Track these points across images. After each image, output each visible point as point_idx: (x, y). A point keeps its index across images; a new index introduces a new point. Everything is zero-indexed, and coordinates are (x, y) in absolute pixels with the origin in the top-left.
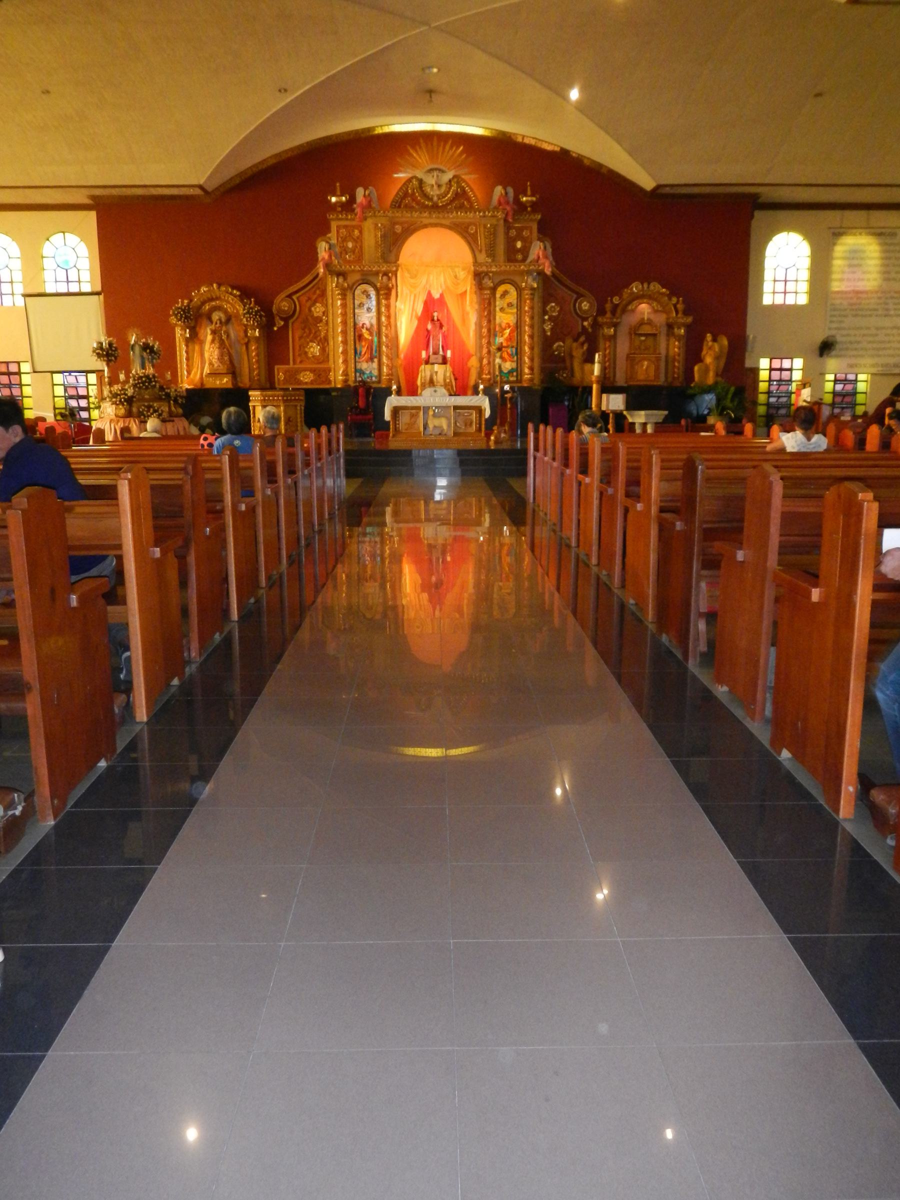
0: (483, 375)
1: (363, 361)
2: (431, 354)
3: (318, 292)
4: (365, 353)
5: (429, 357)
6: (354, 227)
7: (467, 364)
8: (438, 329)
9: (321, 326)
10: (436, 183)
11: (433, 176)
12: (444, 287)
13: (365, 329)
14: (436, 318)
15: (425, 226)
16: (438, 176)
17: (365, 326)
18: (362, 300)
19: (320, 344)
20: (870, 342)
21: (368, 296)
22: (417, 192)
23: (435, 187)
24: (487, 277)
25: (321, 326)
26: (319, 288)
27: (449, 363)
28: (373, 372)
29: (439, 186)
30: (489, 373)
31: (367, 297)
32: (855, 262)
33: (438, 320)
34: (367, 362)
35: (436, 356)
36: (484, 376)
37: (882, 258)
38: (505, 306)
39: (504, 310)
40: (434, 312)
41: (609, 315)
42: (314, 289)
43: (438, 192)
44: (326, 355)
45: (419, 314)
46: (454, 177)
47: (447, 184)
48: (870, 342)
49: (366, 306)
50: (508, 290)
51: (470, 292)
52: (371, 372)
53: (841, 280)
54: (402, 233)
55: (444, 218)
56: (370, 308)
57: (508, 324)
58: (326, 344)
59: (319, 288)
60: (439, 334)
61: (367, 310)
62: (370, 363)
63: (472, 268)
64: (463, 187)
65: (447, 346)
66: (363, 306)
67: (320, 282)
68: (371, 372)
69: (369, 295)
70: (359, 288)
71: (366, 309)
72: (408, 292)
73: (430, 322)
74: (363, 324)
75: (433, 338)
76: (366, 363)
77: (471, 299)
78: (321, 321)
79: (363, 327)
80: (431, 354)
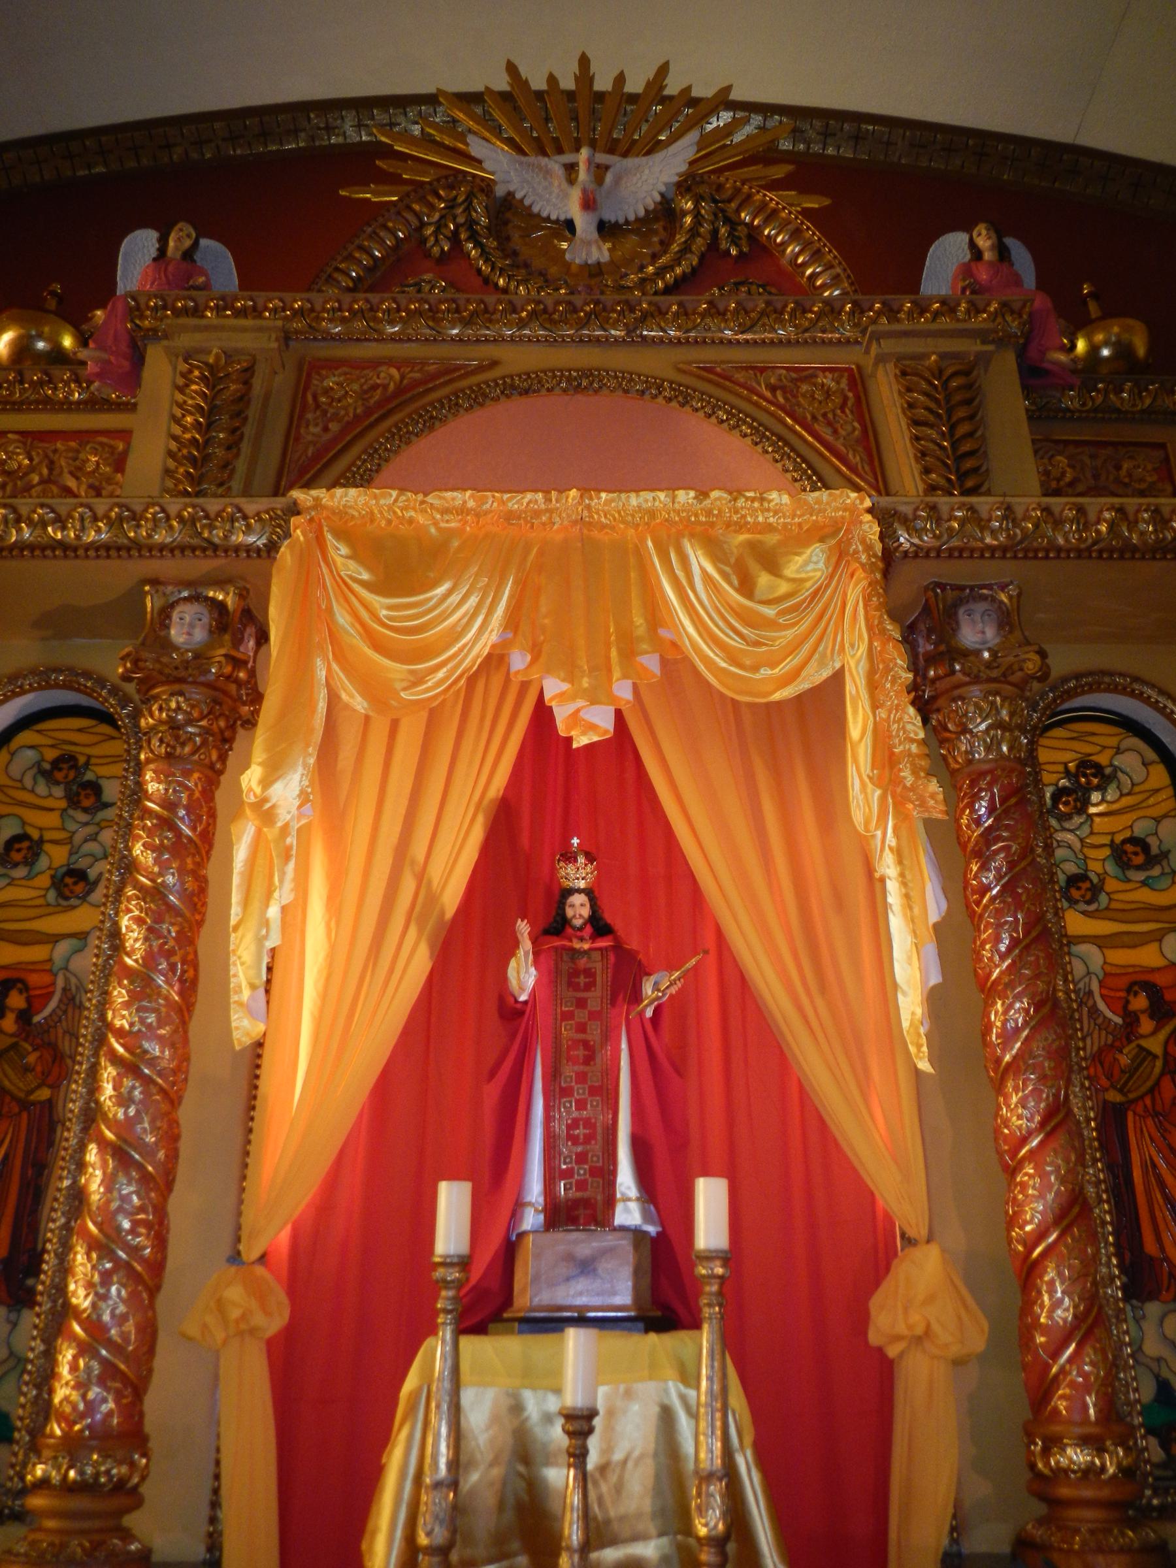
0: (1053, 1443)
2: (531, 1220)
5: (510, 1250)
6: (83, 436)
7: (861, 1320)
8: (595, 998)
10: (588, 204)
11: (571, 168)
12: (651, 662)
14: (578, 908)
16: (600, 171)
17: (16, 1000)
18: (31, 816)
22: (478, 244)
23: (584, 223)
24: (981, 607)
27: (710, 1311)
29: (605, 229)
30: (1110, 1411)
31: (73, 801)
33: (598, 926)
35: (582, 1243)
36: (1076, 1456)
38: (1099, 863)
39: (1096, 890)
40: (570, 857)
43: (600, 253)
45: (451, 897)
46: (687, 184)
47: (649, 218)
49: (57, 856)
50: (1103, 759)
51: (873, 686)
54: (357, 419)
55: (634, 341)
56: (80, 875)
57: (1132, 988)
60: (610, 1036)
61: (58, 883)
63: (871, 529)
64: (750, 226)
65: (679, 1144)
66: (31, 860)
69: (95, 788)
70: (26, 737)
71: (44, 880)
72: (359, 703)
73: (523, 928)
75: (552, 1076)
77: (881, 738)
80: (531, 1220)
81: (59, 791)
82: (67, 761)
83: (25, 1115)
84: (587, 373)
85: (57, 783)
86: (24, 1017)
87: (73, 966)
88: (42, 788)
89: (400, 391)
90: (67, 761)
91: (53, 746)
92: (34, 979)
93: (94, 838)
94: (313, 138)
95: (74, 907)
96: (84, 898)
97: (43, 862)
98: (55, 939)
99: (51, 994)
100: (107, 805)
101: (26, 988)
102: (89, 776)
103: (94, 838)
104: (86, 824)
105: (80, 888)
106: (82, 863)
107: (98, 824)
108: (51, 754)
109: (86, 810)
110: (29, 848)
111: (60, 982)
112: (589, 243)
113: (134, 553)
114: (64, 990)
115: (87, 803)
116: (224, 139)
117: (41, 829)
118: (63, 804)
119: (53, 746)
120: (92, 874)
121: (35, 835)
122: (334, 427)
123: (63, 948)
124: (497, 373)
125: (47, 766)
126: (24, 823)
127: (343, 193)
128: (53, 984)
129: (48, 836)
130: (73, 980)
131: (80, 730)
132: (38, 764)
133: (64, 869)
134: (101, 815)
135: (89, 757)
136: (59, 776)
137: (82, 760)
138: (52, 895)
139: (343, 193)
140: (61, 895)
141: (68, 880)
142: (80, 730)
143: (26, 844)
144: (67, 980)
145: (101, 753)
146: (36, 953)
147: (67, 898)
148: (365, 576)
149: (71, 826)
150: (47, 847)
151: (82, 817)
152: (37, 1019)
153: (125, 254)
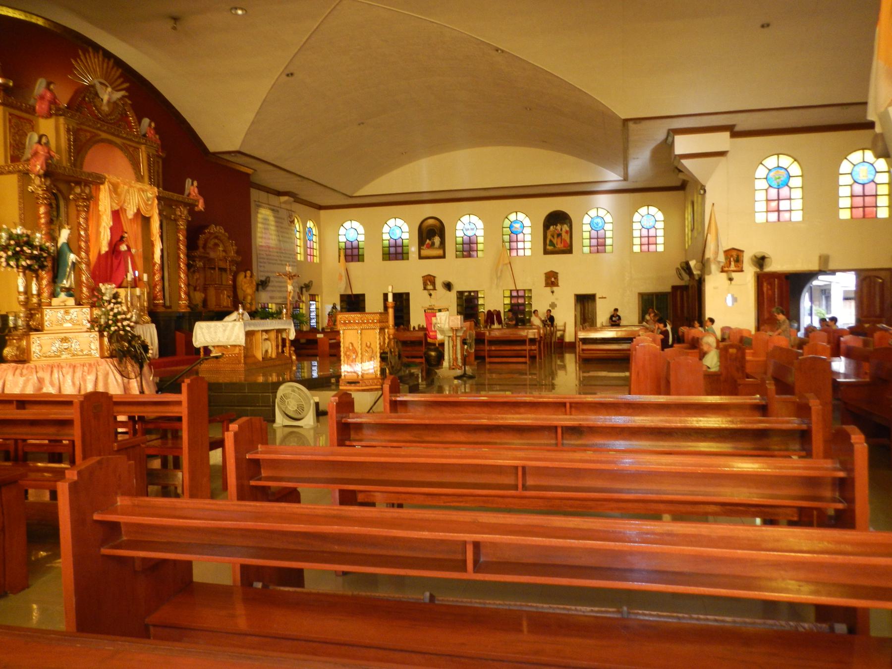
15: (103, 141)
20: (277, 282)
32: (266, 226)
37: (277, 226)
41: (201, 250)
48: (277, 282)
53: (262, 238)
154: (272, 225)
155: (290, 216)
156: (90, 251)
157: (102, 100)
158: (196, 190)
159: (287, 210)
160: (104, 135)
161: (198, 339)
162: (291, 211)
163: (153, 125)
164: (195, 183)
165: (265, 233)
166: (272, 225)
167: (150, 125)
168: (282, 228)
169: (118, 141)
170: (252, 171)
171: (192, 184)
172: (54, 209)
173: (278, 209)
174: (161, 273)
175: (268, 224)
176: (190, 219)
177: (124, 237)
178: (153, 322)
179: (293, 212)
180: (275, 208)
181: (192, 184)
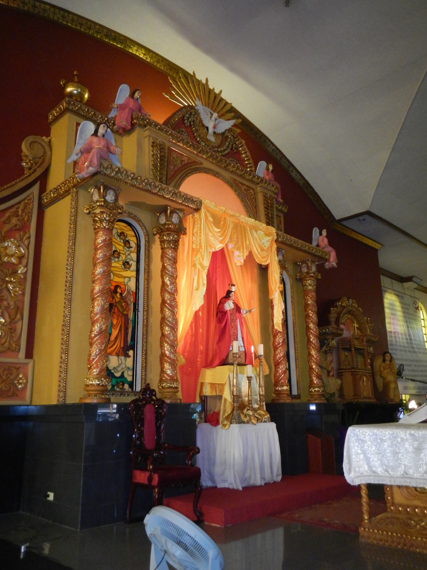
1: (110, 354)
3: (14, 221)
4: (116, 338)
9: (11, 282)
10: (214, 127)
13: (118, 295)
15: (207, 171)
17: (119, 290)
19: (6, 315)
21: (127, 243)
25: (11, 282)
26: (17, 216)
28: (126, 375)
31: (125, 245)
34: (118, 355)
37: (404, 312)
42: (7, 214)
44: (15, 339)
52: (122, 376)
56: (128, 263)
58: (19, 316)
59: (17, 216)
61: (124, 264)
62: (123, 358)
66: (118, 258)
67: (21, 206)
68: (122, 376)
69: (128, 242)
71: (121, 263)
74: (117, 287)
76: (116, 358)
78: (14, 273)
79: (115, 292)
81: (122, 241)
82: (122, 233)
83: (123, 317)
84: (217, 173)
85: (121, 239)
86: (121, 294)
87: (129, 284)
88: (118, 239)
89: (187, 164)
90: (122, 233)
91: (119, 229)
92: (122, 286)
93: (129, 254)
94: (125, 47)
95: (127, 271)
96: (129, 268)
97: (120, 258)
98: (125, 277)
99: (125, 290)
100: (131, 247)
101: (120, 288)
102: (127, 239)
103: (129, 254)
104: (128, 251)
105: (128, 266)
106: (128, 260)
107: (130, 251)
108: (120, 231)
109: (128, 247)
110: (118, 254)
111: (127, 288)
112: (211, 135)
113: (162, 197)
114: (127, 290)
115: (128, 245)
116: (104, 35)
117: (120, 250)
118: (123, 244)
119: (119, 229)
120: (130, 263)
121: (119, 251)
122: (176, 168)
123: (126, 280)
124: (202, 166)
125: (119, 234)
126: (116, 248)
127: (163, 94)
128: (125, 288)
129: (121, 252)
130: (129, 288)
131: (124, 227)
132: (117, 232)
133: (125, 261)
134: (131, 249)
135: (127, 234)
136: (122, 237)
137: (126, 235)
138: (123, 267)
139: (163, 94)
140: (125, 267)
141: (126, 264)
142: (124, 227)
143: (117, 253)
144: (128, 288)
145: (130, 234)
146: (121, 280)
147: (126, 268)
148: (212, 220)
149: (126, 251)
150: (121, 254)
151: (127, 249)
152: (123, 295)
153: (121, 89)
154: (398, 311)
155: (415, 303)
156: (177, 306)
157: (207, 128)
158: (326, 240)
159: (411, 296)
160: (206, 164)
161: (354, 464)
162: (415, 297)
163: (271, 167)
164: (324, 232)
165: (394, 319)
166: (398, 311)
167: (268, 169)
168: (408, 314)
169: (227, 175)
170: (380, 246)
171: (321, 234)
172: (132, 249)
173: (404, 295)
174: (286, 346)
175: (395, 310)
176: (319, 277)
177: (232, 292)
178: (272, 420)
179: (418, 299)
180: (400, 294)
181: (321, 234)
